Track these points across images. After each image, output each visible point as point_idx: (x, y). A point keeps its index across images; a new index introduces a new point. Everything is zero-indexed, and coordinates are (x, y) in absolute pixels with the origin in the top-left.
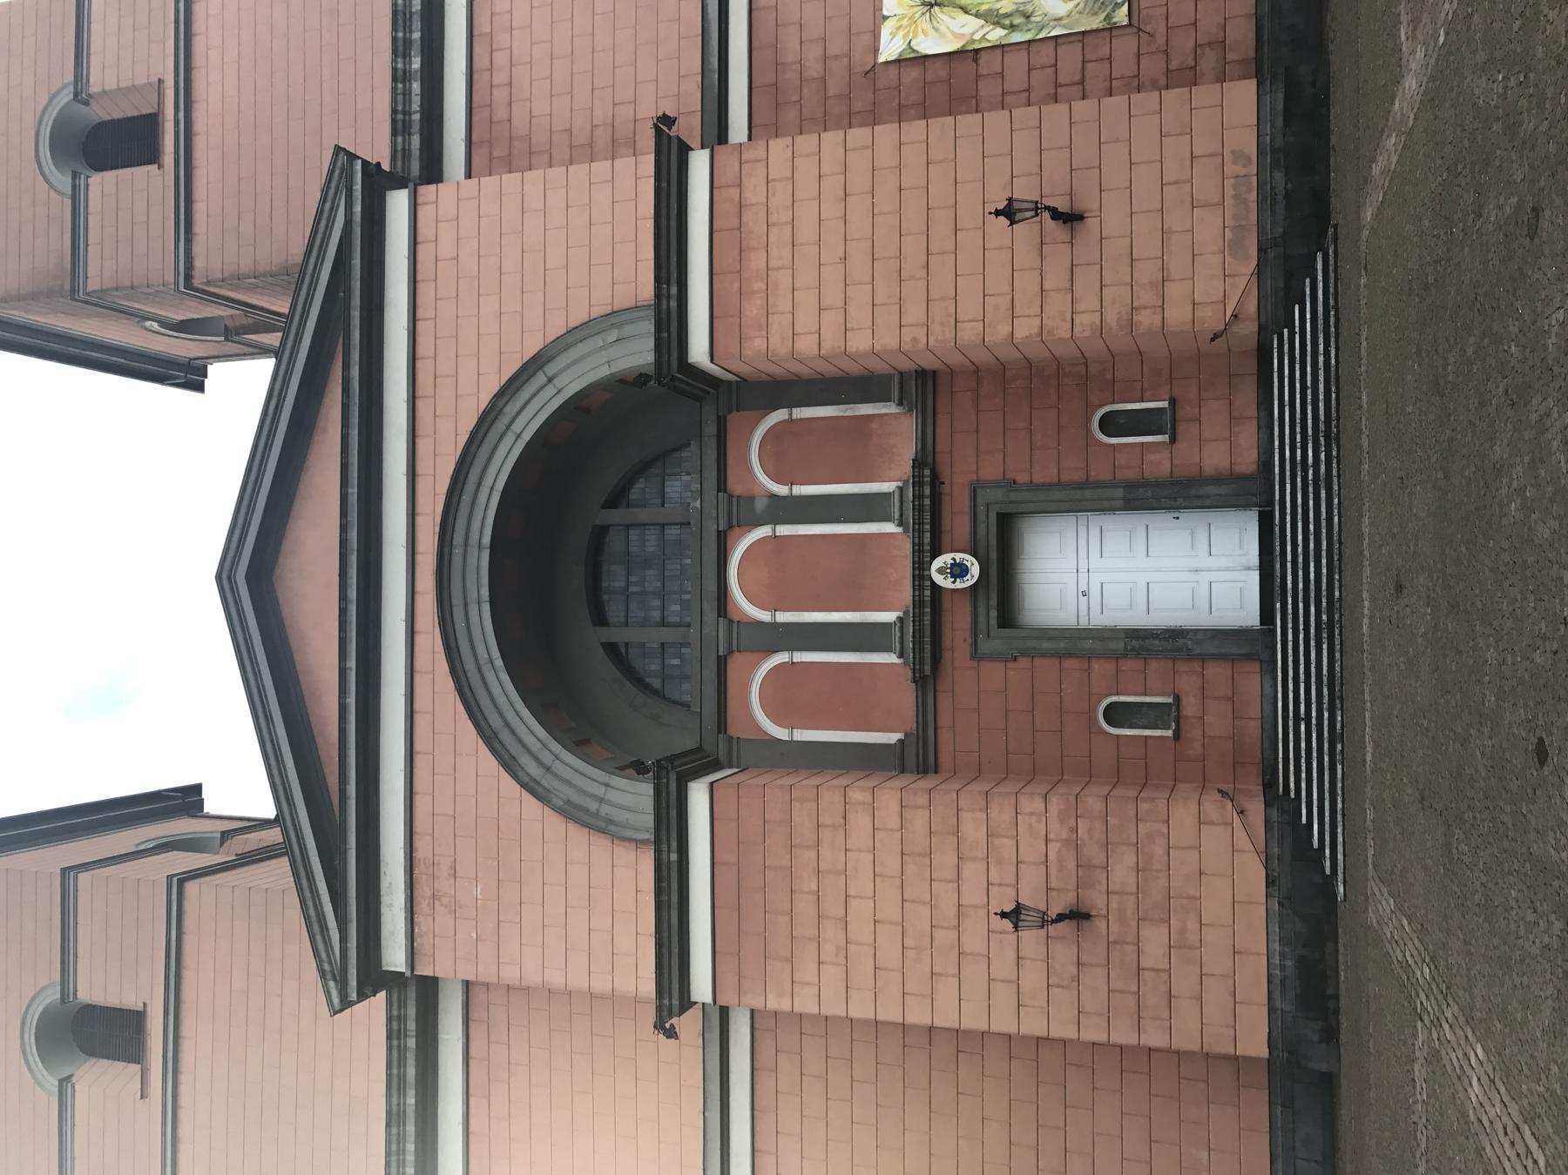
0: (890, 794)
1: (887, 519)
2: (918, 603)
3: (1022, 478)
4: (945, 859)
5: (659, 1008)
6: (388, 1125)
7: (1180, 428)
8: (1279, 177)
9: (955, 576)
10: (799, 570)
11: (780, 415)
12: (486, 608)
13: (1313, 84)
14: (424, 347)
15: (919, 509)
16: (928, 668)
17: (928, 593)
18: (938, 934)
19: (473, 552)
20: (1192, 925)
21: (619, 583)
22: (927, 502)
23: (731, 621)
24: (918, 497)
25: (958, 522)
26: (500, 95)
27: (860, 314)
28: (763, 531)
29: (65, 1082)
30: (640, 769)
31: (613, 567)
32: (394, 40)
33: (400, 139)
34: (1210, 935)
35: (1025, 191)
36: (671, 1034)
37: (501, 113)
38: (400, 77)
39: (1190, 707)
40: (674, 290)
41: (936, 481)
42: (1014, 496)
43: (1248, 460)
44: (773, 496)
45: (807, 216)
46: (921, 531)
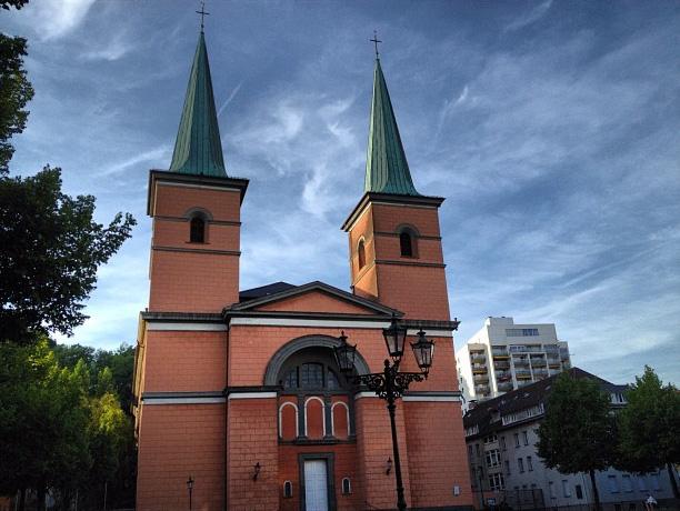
0: (276, 438)
4: (264, 450)
10: (319, 411)
27: (370, 430)
30: (281, 382)
39: (290, 500)
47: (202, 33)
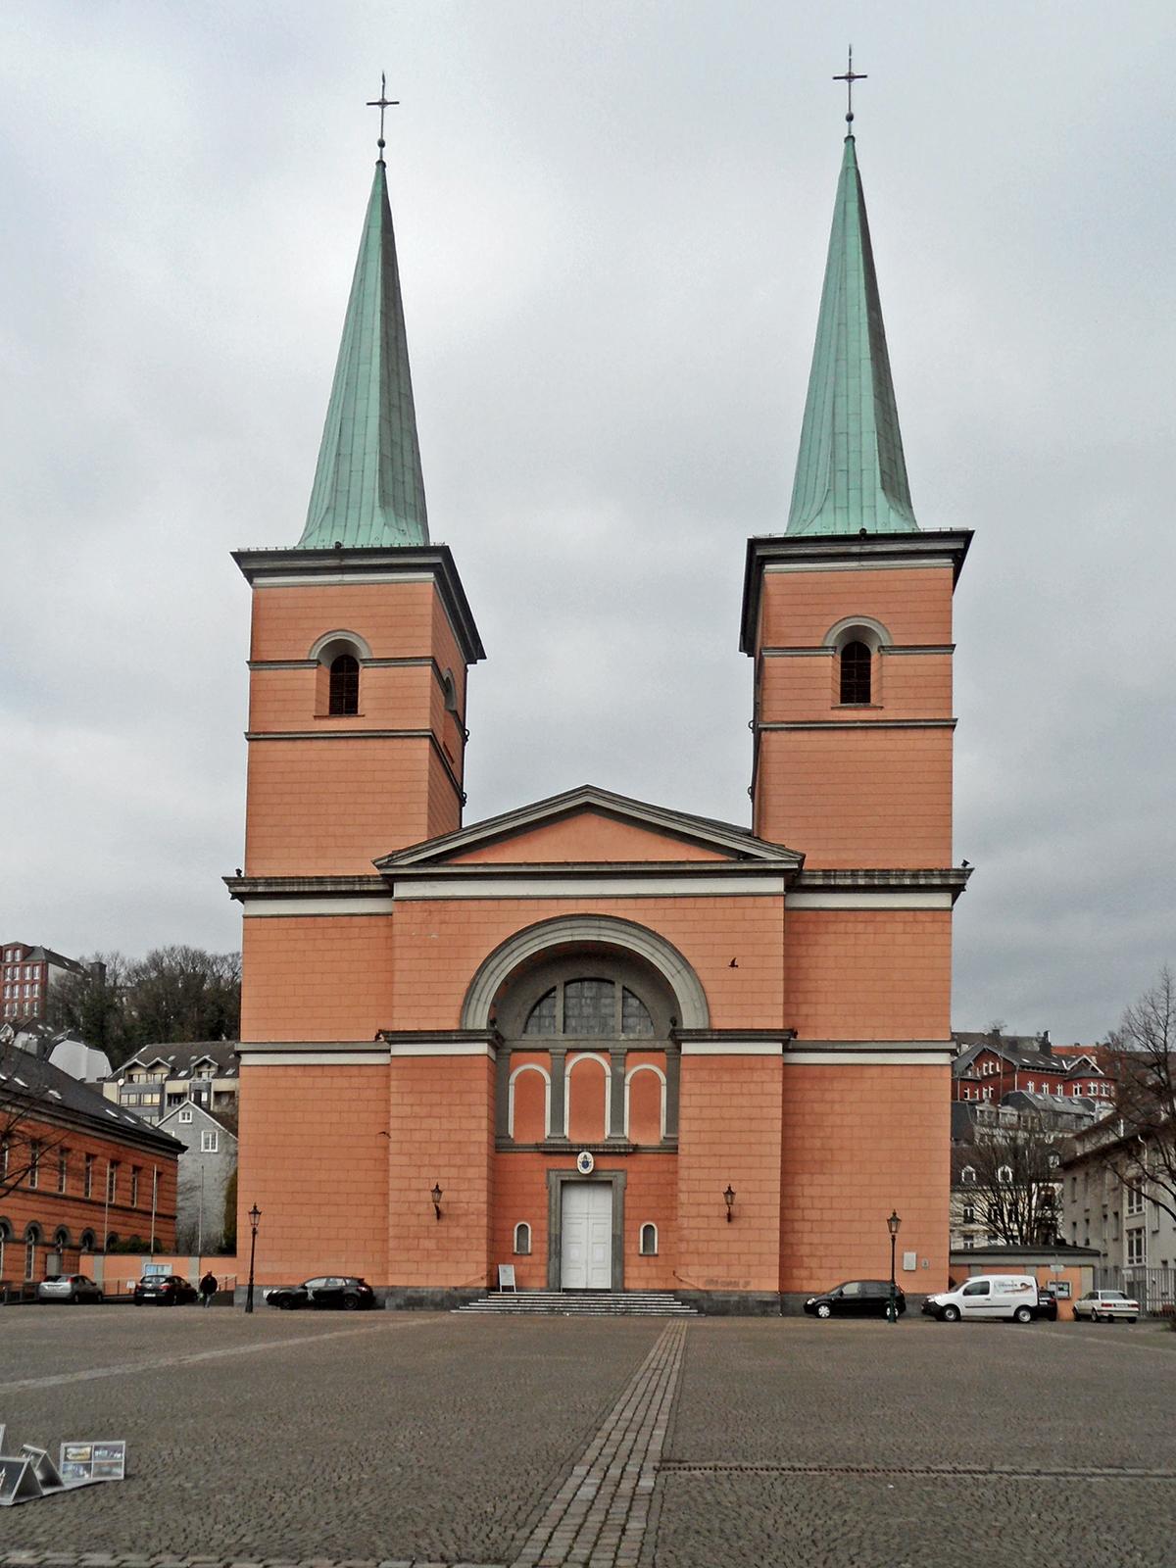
1: (612, 1131)
2: (571, 1146)
3: (627, 1192)
4: (458, 1160)
5: (388, 1032)
6: (317, 877)
7: (645, 1258)
8: (736, 1298)
9: (583, 1163)
11: (664, 1080)
12: (570, 939)
13: (772, 1311)
14: (701, 903)
15: (614, 1147)
16: (542, 1149)
17: (576, 1150)
19: (597, 931)
21: (587, 993)
22: (617, 1150)
23: (566, 1055)
24: (620, 1146)
25: (607, 1163)
26: (841, 927)
28: (608, 1071)
29: (318, 662)
30: (492, 1022)
31: (594, 990)
32: (874, 870)
33: (820, 873)
34: (433, 1266)
36: (377, 1037)
37: (832, 928)
38: (854, 873)
39: (526, 1259)
40: (715, 1037)
41: (627, 1154)
43: (629, 1285)
44: (625, 1076)
45: (744, 1101)
46: (604, 1147)
47: (381, 164)
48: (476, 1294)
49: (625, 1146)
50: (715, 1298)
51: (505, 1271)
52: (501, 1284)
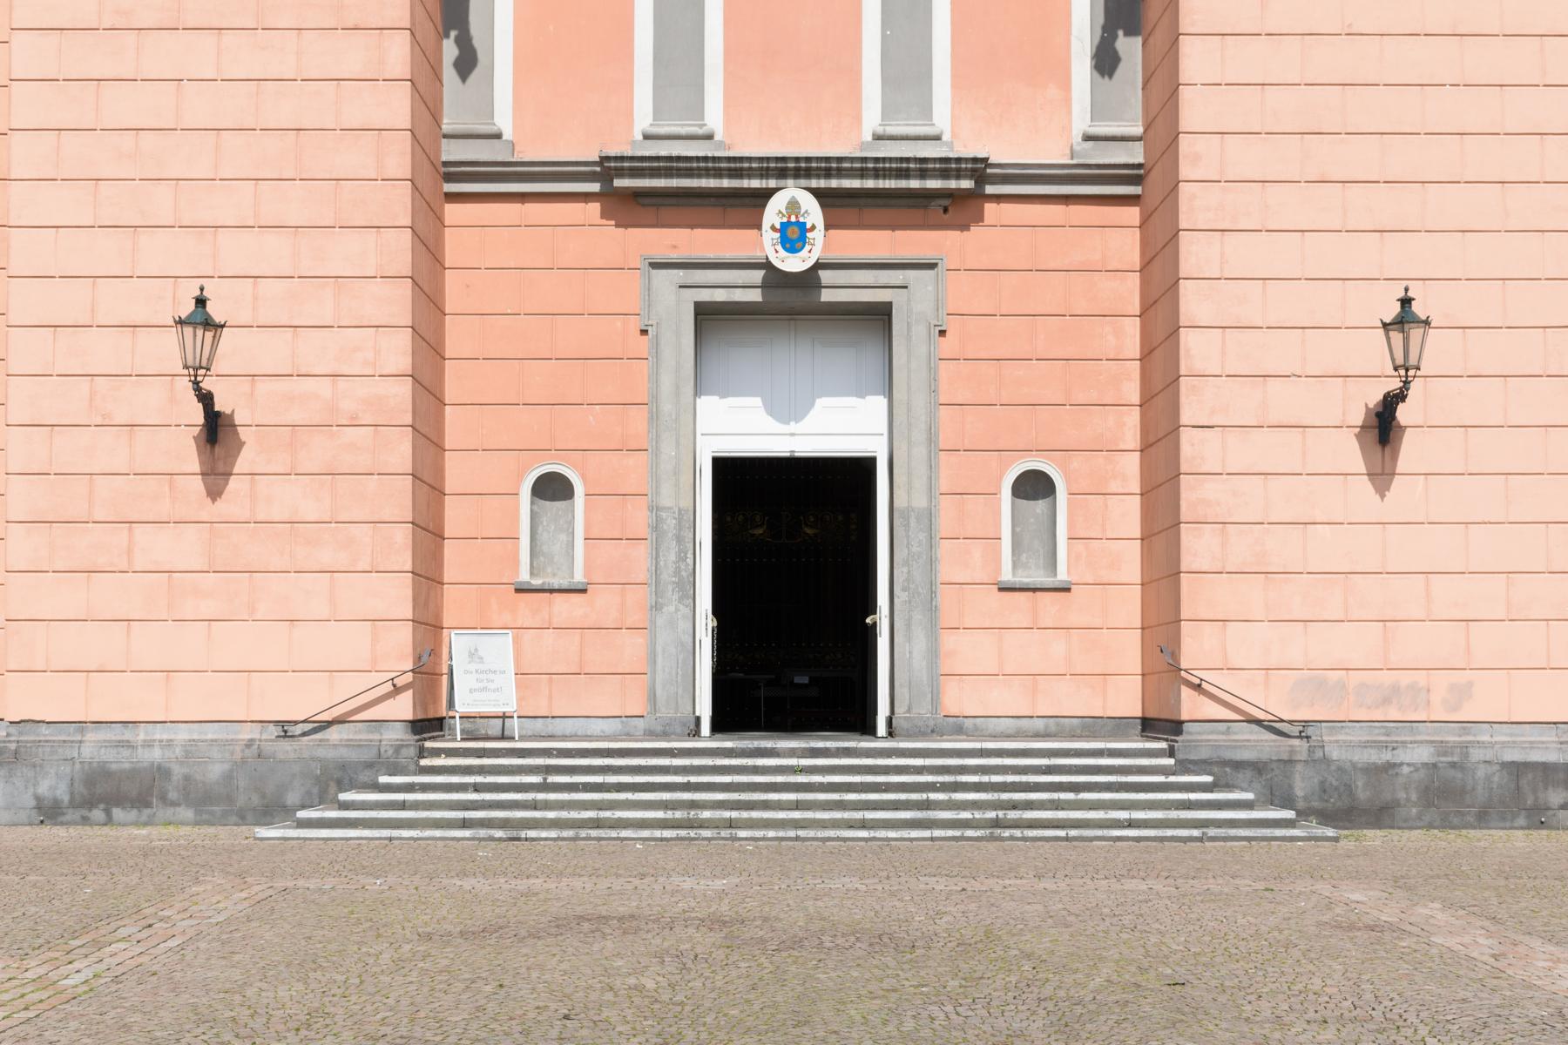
1: (887, 112)
2: (737, 167)
8: (1423, 755)
9: (783, 229)
15: (902, 168)
17: (755, 183)
18: (163, 191)
20: (208, 608)
24: (923, 167)
35: (1436, 351)
42: (919, 331)
48: (367, 755)
49: (948, 167)
50: (1335, 754)
51: (473, 655)
52: (461, 707)
